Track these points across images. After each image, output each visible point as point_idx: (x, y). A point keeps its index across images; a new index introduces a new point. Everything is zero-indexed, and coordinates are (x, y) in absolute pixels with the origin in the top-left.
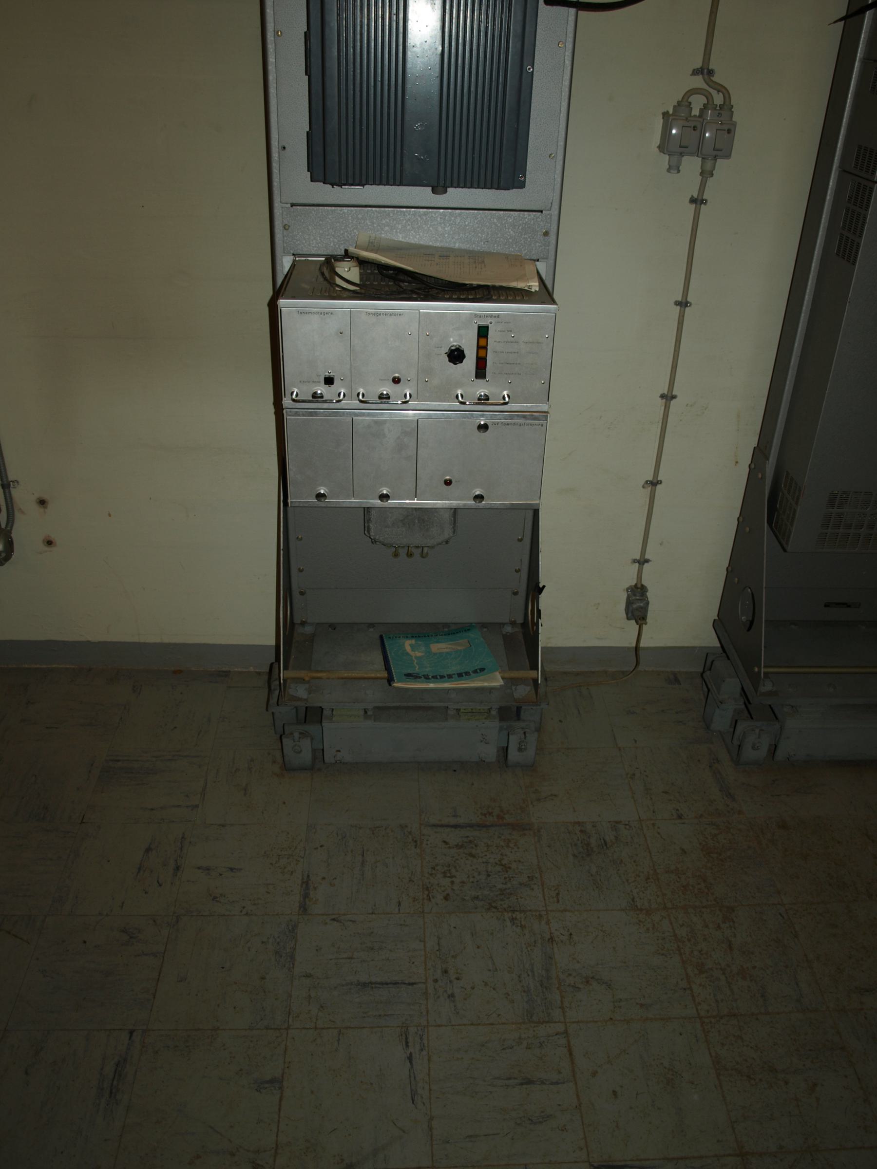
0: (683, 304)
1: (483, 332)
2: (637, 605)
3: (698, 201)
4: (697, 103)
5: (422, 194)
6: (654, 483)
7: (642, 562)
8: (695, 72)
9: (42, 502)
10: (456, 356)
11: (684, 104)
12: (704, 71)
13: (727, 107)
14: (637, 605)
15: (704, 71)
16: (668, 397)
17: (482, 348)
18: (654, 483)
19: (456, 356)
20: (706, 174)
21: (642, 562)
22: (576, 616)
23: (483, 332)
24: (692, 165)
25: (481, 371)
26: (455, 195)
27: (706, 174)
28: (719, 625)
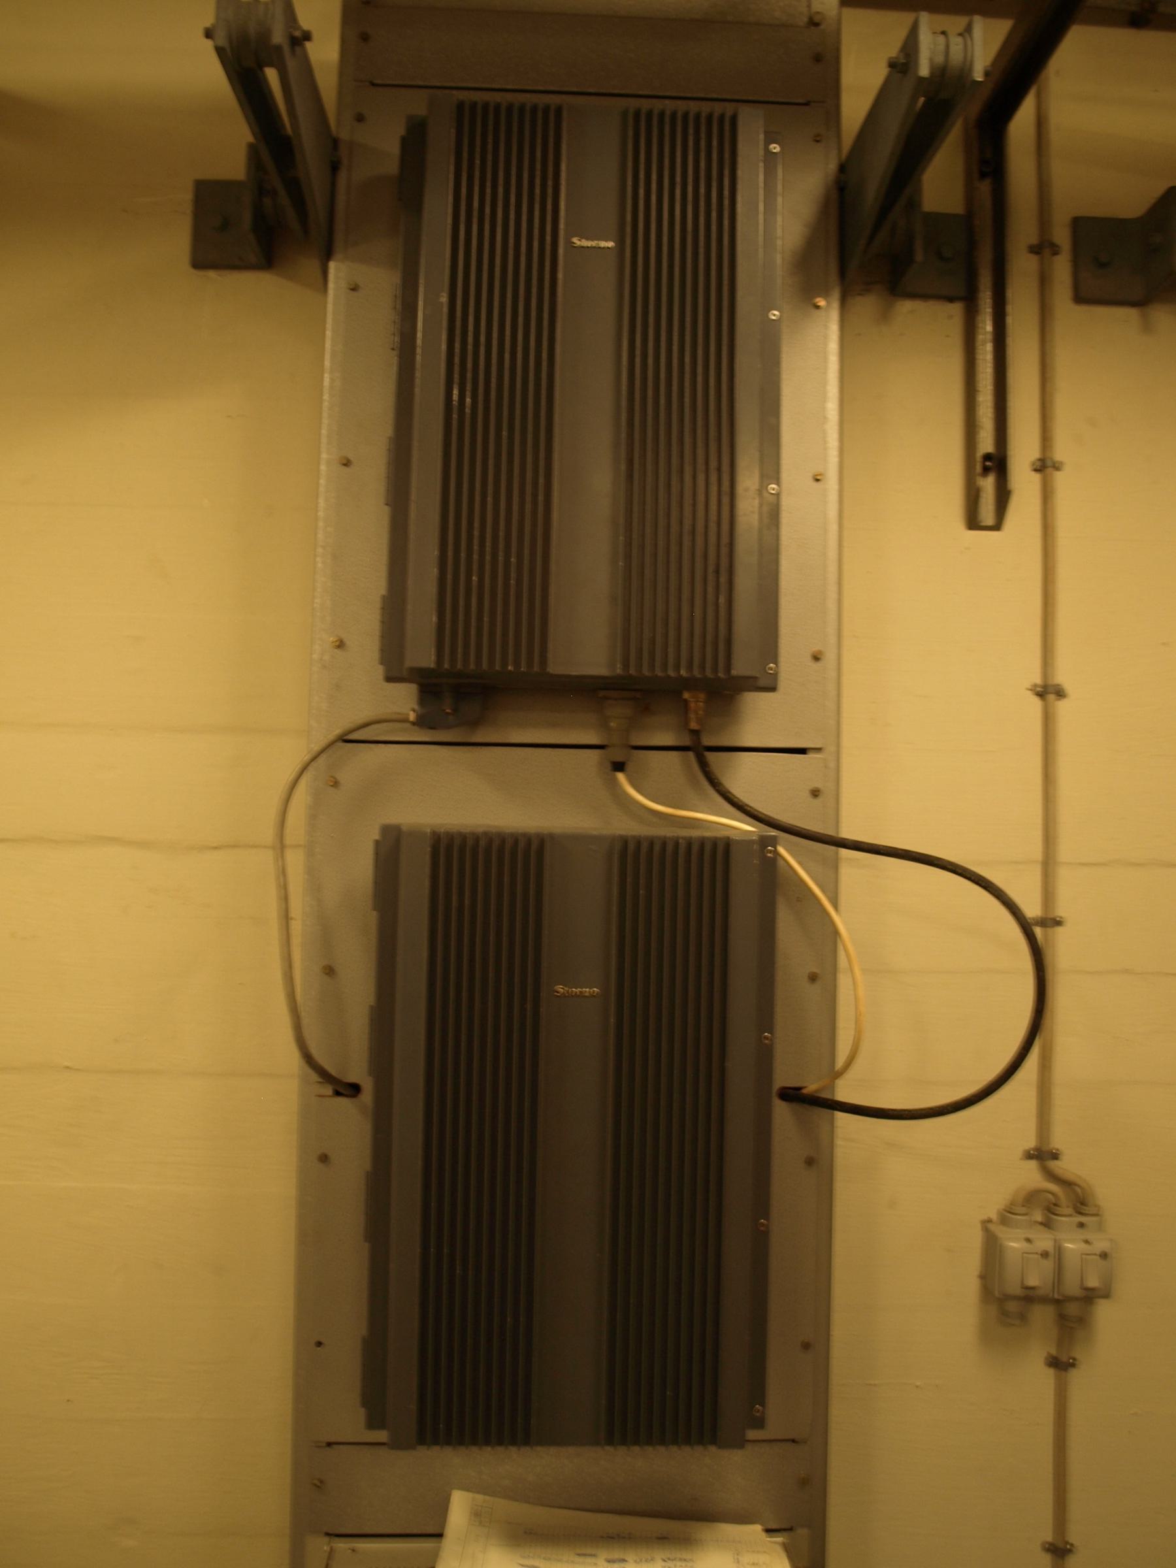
3: (1060, 1364)
8: (1029, 1156)
15: (1043, 1155)
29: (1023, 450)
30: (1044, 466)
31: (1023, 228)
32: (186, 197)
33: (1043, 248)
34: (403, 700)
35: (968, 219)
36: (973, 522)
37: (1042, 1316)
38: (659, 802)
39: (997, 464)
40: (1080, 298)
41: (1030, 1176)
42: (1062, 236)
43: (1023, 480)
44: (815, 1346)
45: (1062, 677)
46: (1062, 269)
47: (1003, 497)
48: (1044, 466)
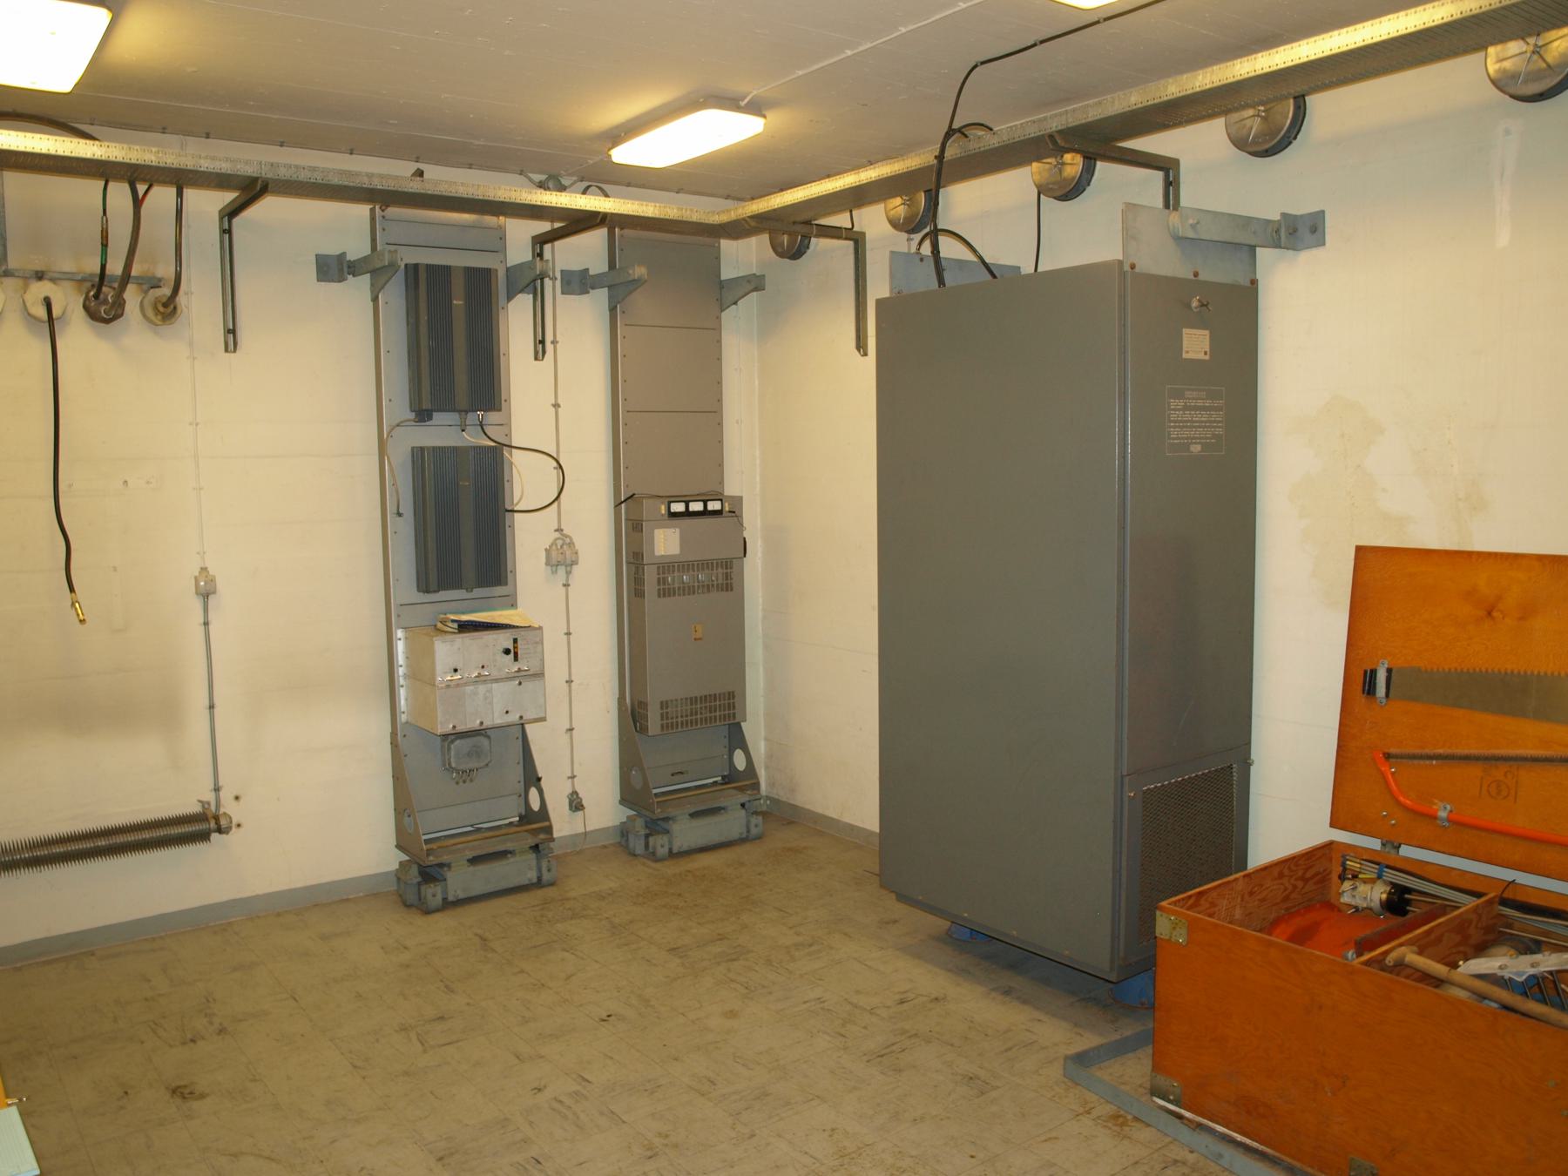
0: (568, 634)
1: (515, 641)
2: (576, 804)
3: (566, 585)
4: (560, 543)
6: (571, 730)
7: (573, 777)
9: (237, 798)
10: (507, 652)
11: (554, 543)
12: (559, 530)
13: (571, 544)
14: (576, 804)
15: (559, 530)
16: (569, 682)
18: (571, 730)
19: (507, 652)
20: (568, 573)
21: (573, 777)
23: (515, 641)
25: (516, 658)
28: (624, 801)
29: (549, 338)
30: (554, 342)
34: (412, 416)
36: (536, 359)
37: (562, 570)
38: (472, 438)
39: (542, 342)
41: (557, 535)
42: (558, 275)
43: (549, 347)
44: (514, 572)
46: (558, 283)
47: (544, 352)
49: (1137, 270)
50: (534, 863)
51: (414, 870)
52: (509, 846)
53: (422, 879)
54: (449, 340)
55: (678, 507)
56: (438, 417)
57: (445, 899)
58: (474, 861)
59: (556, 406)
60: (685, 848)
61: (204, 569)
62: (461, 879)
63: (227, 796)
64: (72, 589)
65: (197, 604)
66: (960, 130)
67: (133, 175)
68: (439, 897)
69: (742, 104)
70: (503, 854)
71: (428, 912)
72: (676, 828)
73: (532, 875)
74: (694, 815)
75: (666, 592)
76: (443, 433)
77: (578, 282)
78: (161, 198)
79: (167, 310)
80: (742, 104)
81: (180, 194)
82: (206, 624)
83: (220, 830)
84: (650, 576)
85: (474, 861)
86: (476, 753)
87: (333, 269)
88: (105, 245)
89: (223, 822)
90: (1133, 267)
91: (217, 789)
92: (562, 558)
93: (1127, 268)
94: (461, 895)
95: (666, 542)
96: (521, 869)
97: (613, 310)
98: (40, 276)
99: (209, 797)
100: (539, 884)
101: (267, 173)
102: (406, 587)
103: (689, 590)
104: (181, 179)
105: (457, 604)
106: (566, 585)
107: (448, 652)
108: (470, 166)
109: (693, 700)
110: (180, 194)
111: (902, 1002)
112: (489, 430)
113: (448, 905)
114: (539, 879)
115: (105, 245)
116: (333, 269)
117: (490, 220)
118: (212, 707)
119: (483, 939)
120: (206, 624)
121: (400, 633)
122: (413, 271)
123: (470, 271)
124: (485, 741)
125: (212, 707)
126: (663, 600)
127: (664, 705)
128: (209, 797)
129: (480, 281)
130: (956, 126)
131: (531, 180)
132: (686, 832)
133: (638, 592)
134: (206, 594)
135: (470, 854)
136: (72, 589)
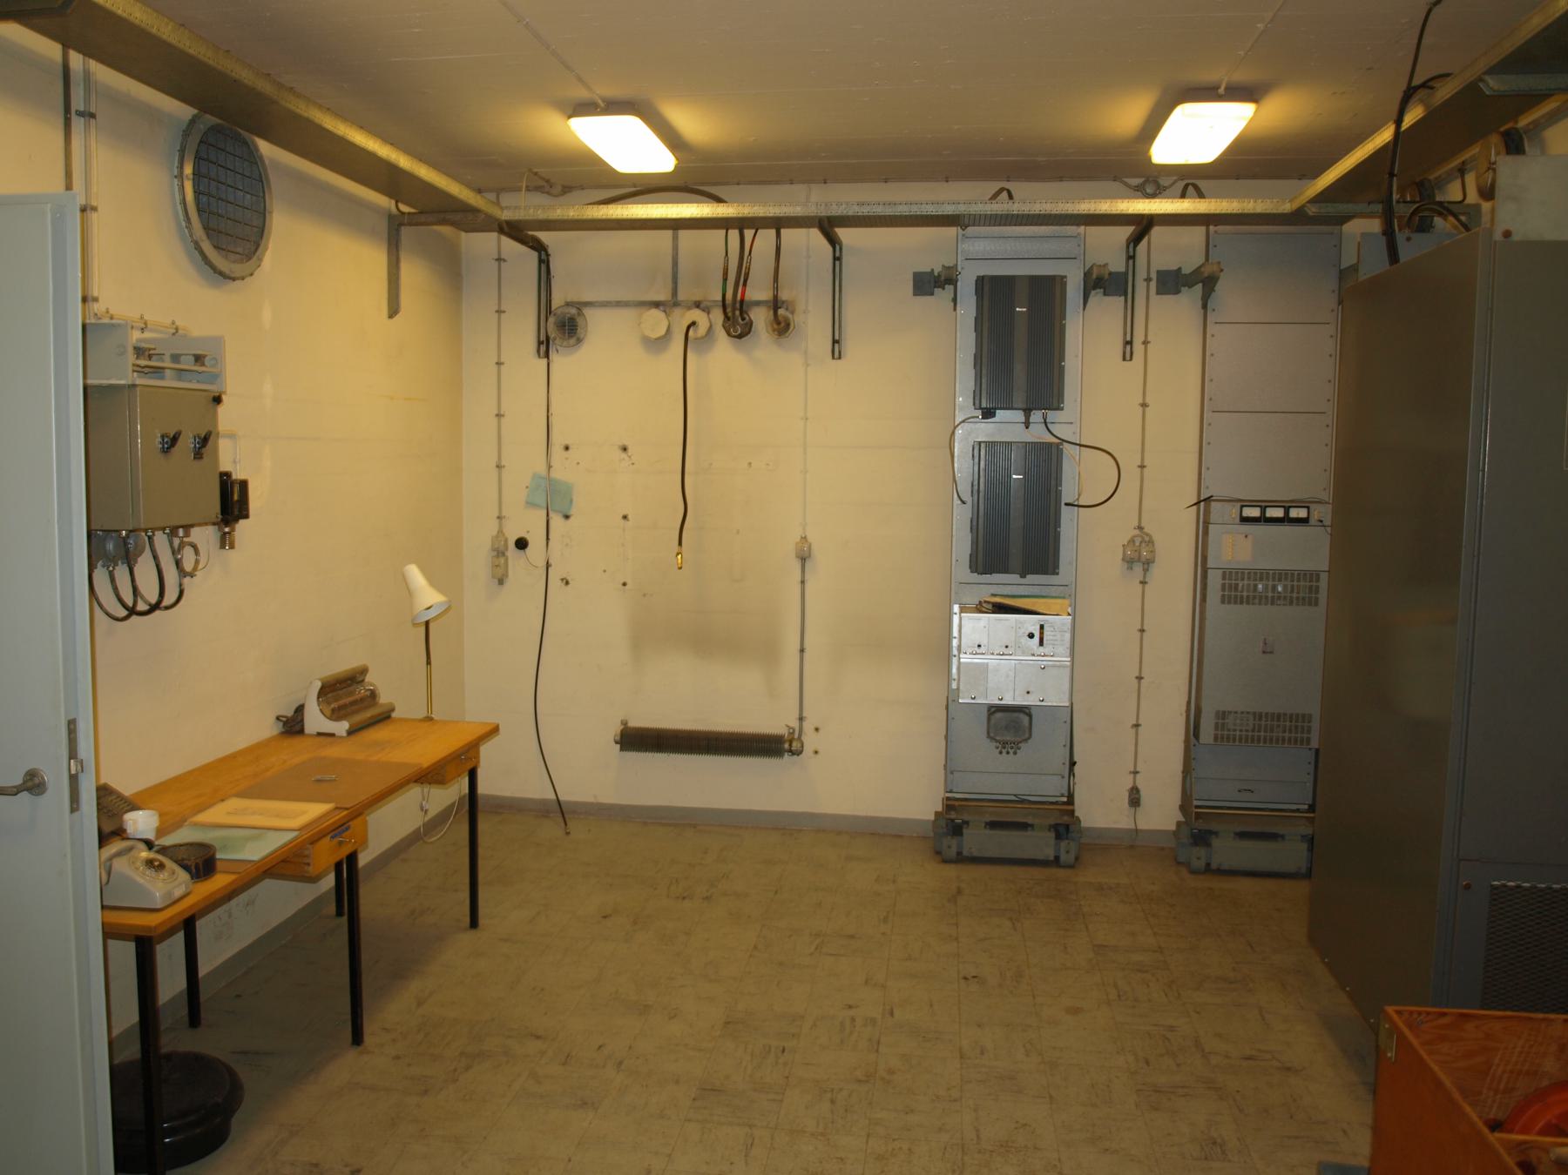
0: (1142, 631)
1: (1042, 627)
2: (1135, 799)
3: (1143, 583)
5: (1015, 578)
6: (1137, 726)
7: (1136, 773)
10: (1031, 636)
11: (1132, 541)
13: (1151, 542)
14: (1135, 799)
15: (1140, 528)
16: (1140, 678)
17: (1042, 633)
18: (1137, 726)
19: (1031, 636)
20: (1146, 571)
22: (1099, 809)
23: (1042, 627)
24: (1138, 568)
25: (1041, 643)
26: (1031, 578)
27: (1146, 571)
30: (1146, 343)
31: (1141, 274)
32: (911, 277)
33: (1148, 280)
34: (979, 413)
35: (1126, 273)
37: (1138, 568)
38: (1037, 434)
39: (1130, 343)
40: (1158, 293)
41: (1137, 532)
42: (1154, 276)
45: (1148, 401)
46: (1153, 284)
48: (1146, 343)
49: (1516, 237)
50: (1052, 841)
51: (943, 823)
52: (1030, 820)
53: (959, 831)
54: (1018, 342)
55: (1254, 512)
56: (1001, 415)
57: (959, 853)
58: (993, 825)
59: (1144, 405)
60: (1226, 866)
61: (804, 538)
62: (976, 839)
63: (808, 727)
64: (680, 543)
65: (797, 565)
66: (1423, 85)
67: (741, 224)
68: (954, 850)
69: (1221, 91)
70: (1024, 826)
71: (945, 861)
72: (1216, 842)
73: (1049, 853)
74: (1242, 835)
75: (1232, 595)
76: (1008, 426)
77: (1171, 282)
78: (766, 237)
79: (782, 327)
80: (1221, 91)
81: (778, 235)
82: (803, 582)
83: (791, 751)
84: (1215, 579)
85: (993, 825)
86: (1015, 727)
87: (926, 284)
88: (725, 279)
89: (795, 745)
90: (1507, 234)
91: (801, 719)
92: (1140, 557)
93: (1498, 236)
94: (976, 854)
95: (1236, 547)
96: (1040, 844)
97: (1205, 307)
98: (697, 305)
99: (795, 724)
100: (1056, 862)
101: (835, 211)
102: (963, 571)
103: (1262, 600)
104: (778, 224)
105: (1004, 585)
106: (1143, 583)
107: (973, 628)
108: (1061, 179)
109: (1259, 716)
110: (778, 235)
111: (1249, 1058)
112: (1054, 429)
113: (961, 859)
114: (1057, 858)
115: (725, 279)
116: (926, 284)
117: (1070, 230)
118: (802, 651)
119: (959, 891)
120: (803, 582)
121: (956, 608)
122: (980, 281)
123: (1035, 281)
124: (1026, 719)
125: (802, 651)
126: (1227, 606)
127: (1222, 715)
128: (795, 724)
129: (1046, 292)
130: (1416, 82)
131: (1126, 184)
132: (1227, 851)
133: (1204, 599)
134: (804, 559)
135: (989, 818)
136: (680, 543)
